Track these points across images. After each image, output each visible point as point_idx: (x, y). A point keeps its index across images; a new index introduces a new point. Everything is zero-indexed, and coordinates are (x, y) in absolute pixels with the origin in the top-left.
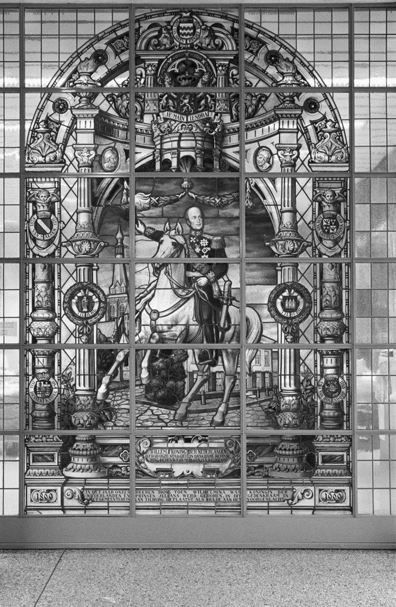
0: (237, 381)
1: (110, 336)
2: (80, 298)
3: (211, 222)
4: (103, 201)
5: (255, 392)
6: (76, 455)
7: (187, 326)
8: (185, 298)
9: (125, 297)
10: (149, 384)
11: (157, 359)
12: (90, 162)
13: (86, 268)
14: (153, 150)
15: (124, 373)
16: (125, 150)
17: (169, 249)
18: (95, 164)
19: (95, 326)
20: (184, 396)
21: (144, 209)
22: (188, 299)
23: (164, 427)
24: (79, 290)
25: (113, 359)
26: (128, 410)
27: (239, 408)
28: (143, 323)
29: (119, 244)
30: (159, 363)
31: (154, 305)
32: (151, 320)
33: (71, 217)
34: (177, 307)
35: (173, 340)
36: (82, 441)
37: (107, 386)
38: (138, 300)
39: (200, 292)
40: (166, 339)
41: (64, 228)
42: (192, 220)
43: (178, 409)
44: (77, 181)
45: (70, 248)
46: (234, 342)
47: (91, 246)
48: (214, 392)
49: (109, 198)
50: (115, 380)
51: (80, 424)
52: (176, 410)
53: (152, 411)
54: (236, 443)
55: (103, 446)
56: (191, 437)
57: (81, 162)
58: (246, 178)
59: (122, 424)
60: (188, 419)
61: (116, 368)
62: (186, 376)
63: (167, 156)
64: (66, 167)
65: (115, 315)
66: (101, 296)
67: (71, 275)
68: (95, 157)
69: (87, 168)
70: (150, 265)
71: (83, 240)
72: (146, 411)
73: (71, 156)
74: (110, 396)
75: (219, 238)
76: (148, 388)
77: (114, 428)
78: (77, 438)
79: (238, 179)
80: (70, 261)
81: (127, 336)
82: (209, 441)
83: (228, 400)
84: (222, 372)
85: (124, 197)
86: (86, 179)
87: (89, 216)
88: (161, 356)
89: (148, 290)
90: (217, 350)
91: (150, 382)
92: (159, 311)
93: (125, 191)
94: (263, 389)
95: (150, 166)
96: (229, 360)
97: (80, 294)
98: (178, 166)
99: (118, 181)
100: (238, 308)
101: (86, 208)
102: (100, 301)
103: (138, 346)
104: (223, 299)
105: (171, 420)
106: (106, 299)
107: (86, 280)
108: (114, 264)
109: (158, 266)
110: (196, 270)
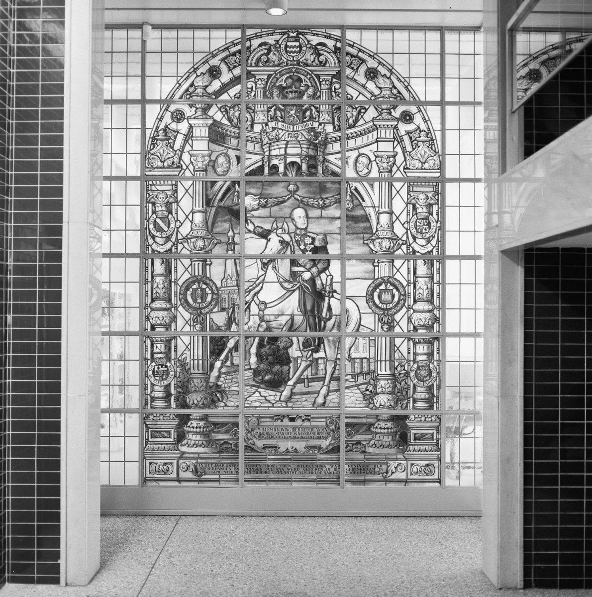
0: (338, 366)
1: (222, 324)
2: (194, 290)
3: (315, 222)
4: (216, 202)
5: (353, 376)
6: (190, 432)
7: (292, 317)
8: (290, 291)
9: (235, 289)
10: (257, 368)
11: (264, 346)
12: (204, 167)
13: (201, 263)
14: (262, 156)
15: (235, 358)
16: (236, 156)
17: (276, 247)
18: (209, 168)
19: (208, 316)
20: (289, 379)
21: (254, 210)
22: (294, 291)
23: (271, 407)
24: (194, 283)
25: (224, 345)
26: (238, 391)
27: (338, 390)
28: (251, 314)
29: (230, 241)
30: (266, 350)
31: (262, 296)
32: (260, 310)
33: (187, 217)
34: (283, 299)
35: (280, 329)
36: (196, 419)
37: (219, 371)
38: (247, 292)
39: (304, 285)
40: (273, 328)
41: (180, 226)
42: (296, 219)
43: (283, 391)
44: (193, 184)
45: (186, 245)
46: (335, 331)
47: (204, 243)
48: (316, 376)
49: (221, 200)
50: (226, 364)
51: (194, 404)
52: (282, 392)
53: (260, 392)
54: (336, 421)
55: (215, 424)
56: (295, 416)
57: (196, 167)
58: (347, 182)
59: (232, 404)
60: (292, 400)
61: (227, 354)
62: (291, 362)
63: (275, 162)
64: (183, 171)
65: (227, 306)
66: (214, 288)
67: (187, 269)
68: (209, 163)
69: (202, 173)
70: (259, 260)
71: (198, 237)
72: (254, 393)
73: (187, 162)
74: (222, 379)
75: (322, 236)
76: (256, 372)
77: (225, 408)
78: (191, 417)
79: (339, 183)
80: (185, 257)
81: (237, 325)
82: (312, 420)
83: (329, 383)
84: (324, 358)
85: (236, 198)
86: (201, 182)
87: (203, 215)
88: (267, 342)
89: (257, 283)
90: (319, 338)
91: (258, 366)
92: (267, 302)
93: (236, 193)
94: (361, 373)
95: (260, 170)
96: (330, 348)
97: (194, 287)
98: (285, 171)
99: (229, 185)
100: (339, 300)
101: (201, 209)
102: (213, 293)
103: (248, 334)
104: (325, 291)
105: (277, 402)
106: (218, 291)
107: (200, 274)
108: (226, 259)
109: (266, 262)
110: (301, 265)
